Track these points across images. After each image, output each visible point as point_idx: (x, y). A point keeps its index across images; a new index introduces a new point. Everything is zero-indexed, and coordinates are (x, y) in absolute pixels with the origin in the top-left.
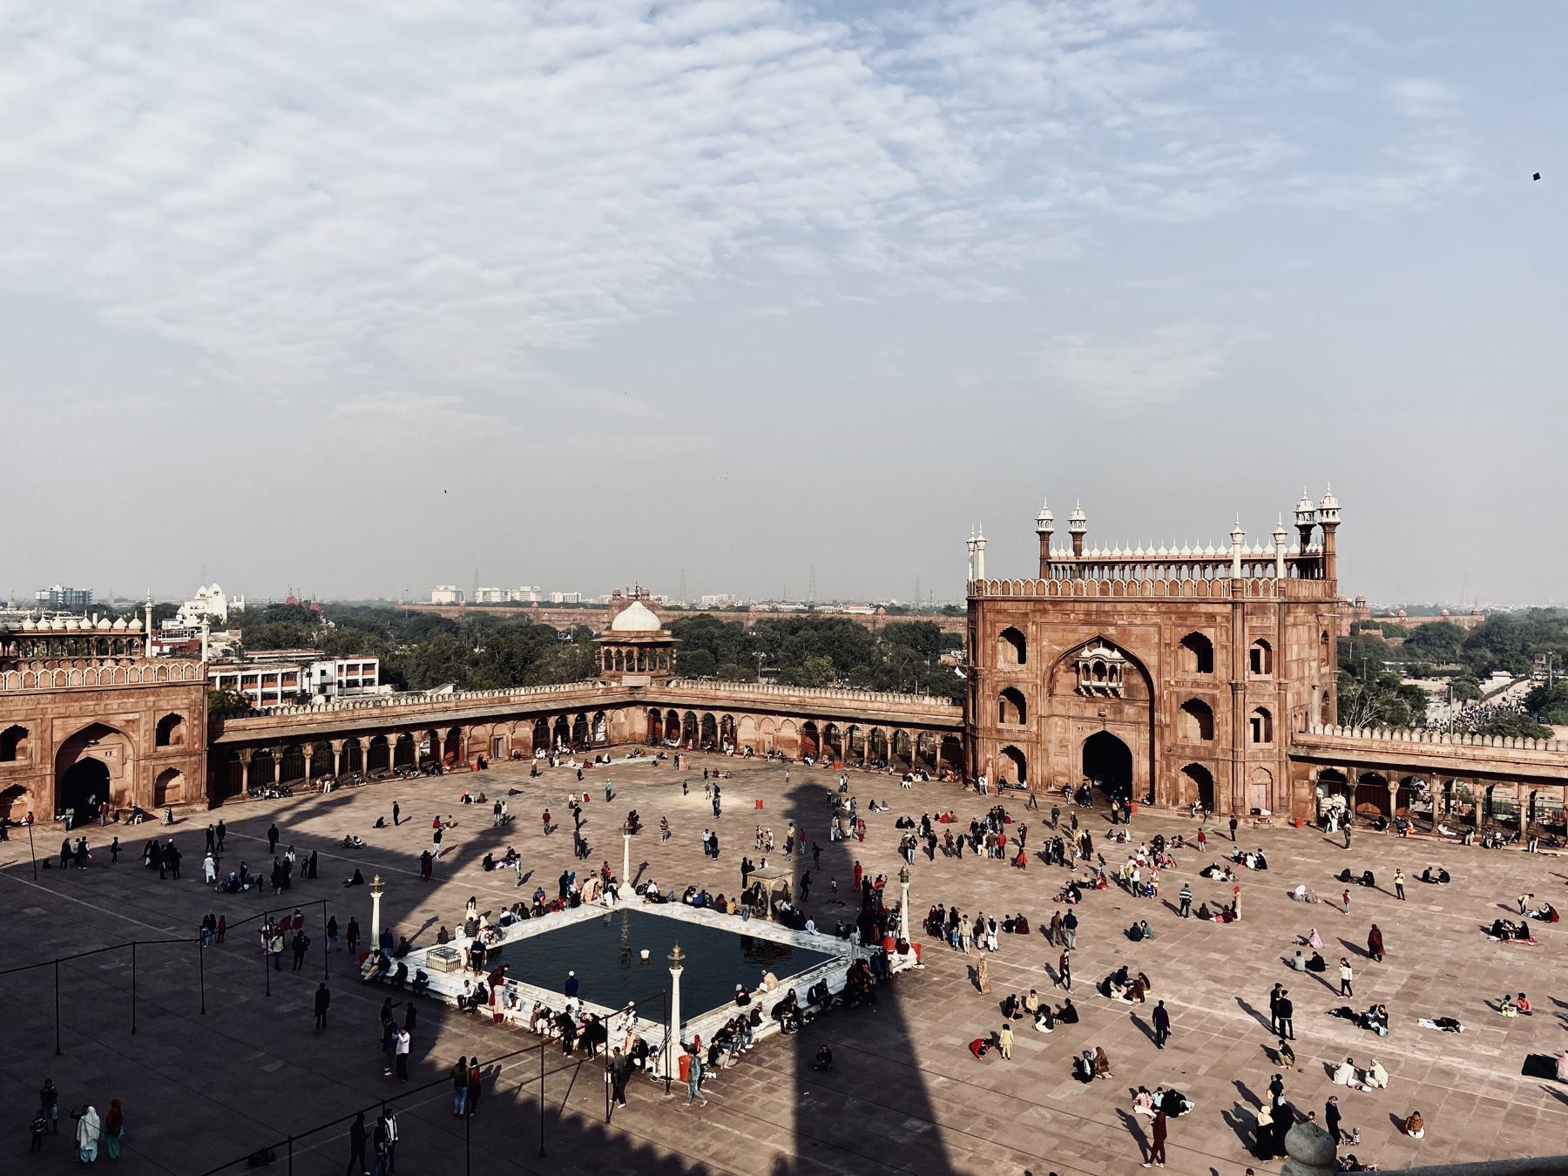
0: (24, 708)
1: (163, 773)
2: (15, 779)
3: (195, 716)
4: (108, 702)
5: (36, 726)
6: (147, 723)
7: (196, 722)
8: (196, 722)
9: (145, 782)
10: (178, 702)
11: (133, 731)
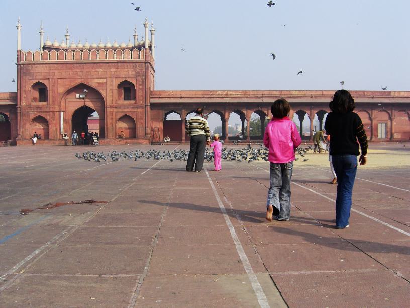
0: (44, 71)
2: (39, 112)
7: (141, 87)
8: (141, 87)
9: (111, 121)
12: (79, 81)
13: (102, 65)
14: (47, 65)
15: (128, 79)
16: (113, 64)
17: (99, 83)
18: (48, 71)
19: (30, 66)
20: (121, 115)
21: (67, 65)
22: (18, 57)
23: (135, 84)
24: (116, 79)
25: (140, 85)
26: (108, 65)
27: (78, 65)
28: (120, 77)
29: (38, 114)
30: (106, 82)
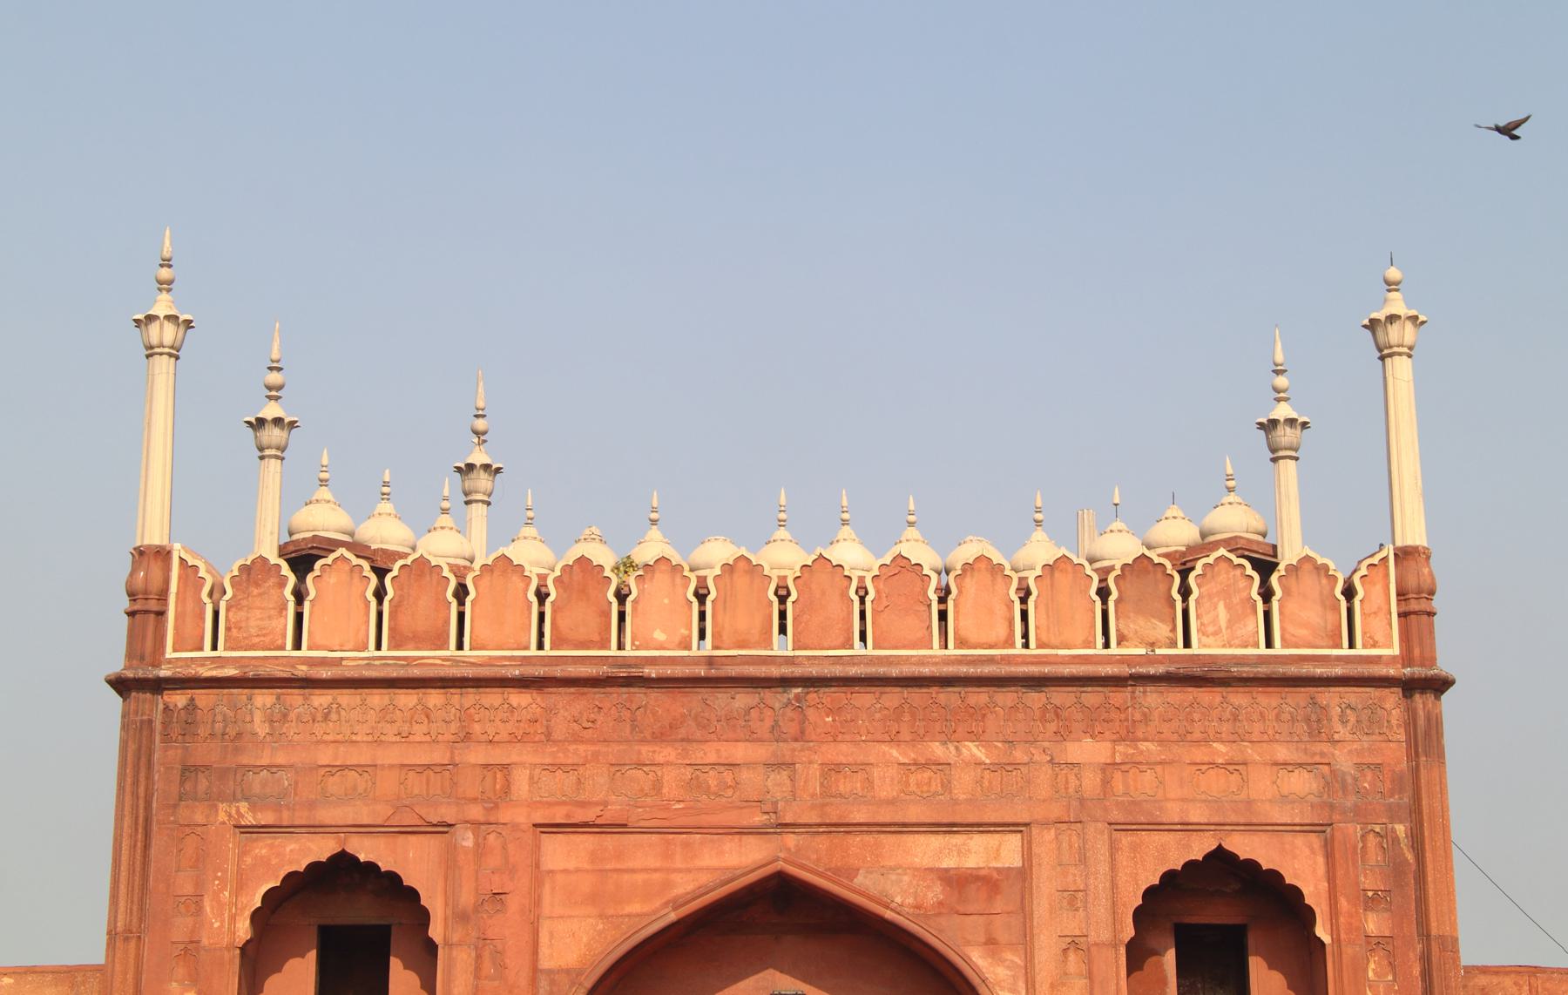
3: (1370, 882)
6: (1073, 898)
7: (1374, 924)
8: (1374, 924)
10: (1262, 785)
11: (991, 943)
13: (979, 697)
14: (435, 698)
15: (1244, 847)
16: (1092, 697)
17: (958, 881)
18: (438, 756)
19: (264, 698)
21: (639, 695)
23: (1314, 892)
24: (1126, 840)
26: (1035, 698)
27: (743, 699)
30: (1024, 874)
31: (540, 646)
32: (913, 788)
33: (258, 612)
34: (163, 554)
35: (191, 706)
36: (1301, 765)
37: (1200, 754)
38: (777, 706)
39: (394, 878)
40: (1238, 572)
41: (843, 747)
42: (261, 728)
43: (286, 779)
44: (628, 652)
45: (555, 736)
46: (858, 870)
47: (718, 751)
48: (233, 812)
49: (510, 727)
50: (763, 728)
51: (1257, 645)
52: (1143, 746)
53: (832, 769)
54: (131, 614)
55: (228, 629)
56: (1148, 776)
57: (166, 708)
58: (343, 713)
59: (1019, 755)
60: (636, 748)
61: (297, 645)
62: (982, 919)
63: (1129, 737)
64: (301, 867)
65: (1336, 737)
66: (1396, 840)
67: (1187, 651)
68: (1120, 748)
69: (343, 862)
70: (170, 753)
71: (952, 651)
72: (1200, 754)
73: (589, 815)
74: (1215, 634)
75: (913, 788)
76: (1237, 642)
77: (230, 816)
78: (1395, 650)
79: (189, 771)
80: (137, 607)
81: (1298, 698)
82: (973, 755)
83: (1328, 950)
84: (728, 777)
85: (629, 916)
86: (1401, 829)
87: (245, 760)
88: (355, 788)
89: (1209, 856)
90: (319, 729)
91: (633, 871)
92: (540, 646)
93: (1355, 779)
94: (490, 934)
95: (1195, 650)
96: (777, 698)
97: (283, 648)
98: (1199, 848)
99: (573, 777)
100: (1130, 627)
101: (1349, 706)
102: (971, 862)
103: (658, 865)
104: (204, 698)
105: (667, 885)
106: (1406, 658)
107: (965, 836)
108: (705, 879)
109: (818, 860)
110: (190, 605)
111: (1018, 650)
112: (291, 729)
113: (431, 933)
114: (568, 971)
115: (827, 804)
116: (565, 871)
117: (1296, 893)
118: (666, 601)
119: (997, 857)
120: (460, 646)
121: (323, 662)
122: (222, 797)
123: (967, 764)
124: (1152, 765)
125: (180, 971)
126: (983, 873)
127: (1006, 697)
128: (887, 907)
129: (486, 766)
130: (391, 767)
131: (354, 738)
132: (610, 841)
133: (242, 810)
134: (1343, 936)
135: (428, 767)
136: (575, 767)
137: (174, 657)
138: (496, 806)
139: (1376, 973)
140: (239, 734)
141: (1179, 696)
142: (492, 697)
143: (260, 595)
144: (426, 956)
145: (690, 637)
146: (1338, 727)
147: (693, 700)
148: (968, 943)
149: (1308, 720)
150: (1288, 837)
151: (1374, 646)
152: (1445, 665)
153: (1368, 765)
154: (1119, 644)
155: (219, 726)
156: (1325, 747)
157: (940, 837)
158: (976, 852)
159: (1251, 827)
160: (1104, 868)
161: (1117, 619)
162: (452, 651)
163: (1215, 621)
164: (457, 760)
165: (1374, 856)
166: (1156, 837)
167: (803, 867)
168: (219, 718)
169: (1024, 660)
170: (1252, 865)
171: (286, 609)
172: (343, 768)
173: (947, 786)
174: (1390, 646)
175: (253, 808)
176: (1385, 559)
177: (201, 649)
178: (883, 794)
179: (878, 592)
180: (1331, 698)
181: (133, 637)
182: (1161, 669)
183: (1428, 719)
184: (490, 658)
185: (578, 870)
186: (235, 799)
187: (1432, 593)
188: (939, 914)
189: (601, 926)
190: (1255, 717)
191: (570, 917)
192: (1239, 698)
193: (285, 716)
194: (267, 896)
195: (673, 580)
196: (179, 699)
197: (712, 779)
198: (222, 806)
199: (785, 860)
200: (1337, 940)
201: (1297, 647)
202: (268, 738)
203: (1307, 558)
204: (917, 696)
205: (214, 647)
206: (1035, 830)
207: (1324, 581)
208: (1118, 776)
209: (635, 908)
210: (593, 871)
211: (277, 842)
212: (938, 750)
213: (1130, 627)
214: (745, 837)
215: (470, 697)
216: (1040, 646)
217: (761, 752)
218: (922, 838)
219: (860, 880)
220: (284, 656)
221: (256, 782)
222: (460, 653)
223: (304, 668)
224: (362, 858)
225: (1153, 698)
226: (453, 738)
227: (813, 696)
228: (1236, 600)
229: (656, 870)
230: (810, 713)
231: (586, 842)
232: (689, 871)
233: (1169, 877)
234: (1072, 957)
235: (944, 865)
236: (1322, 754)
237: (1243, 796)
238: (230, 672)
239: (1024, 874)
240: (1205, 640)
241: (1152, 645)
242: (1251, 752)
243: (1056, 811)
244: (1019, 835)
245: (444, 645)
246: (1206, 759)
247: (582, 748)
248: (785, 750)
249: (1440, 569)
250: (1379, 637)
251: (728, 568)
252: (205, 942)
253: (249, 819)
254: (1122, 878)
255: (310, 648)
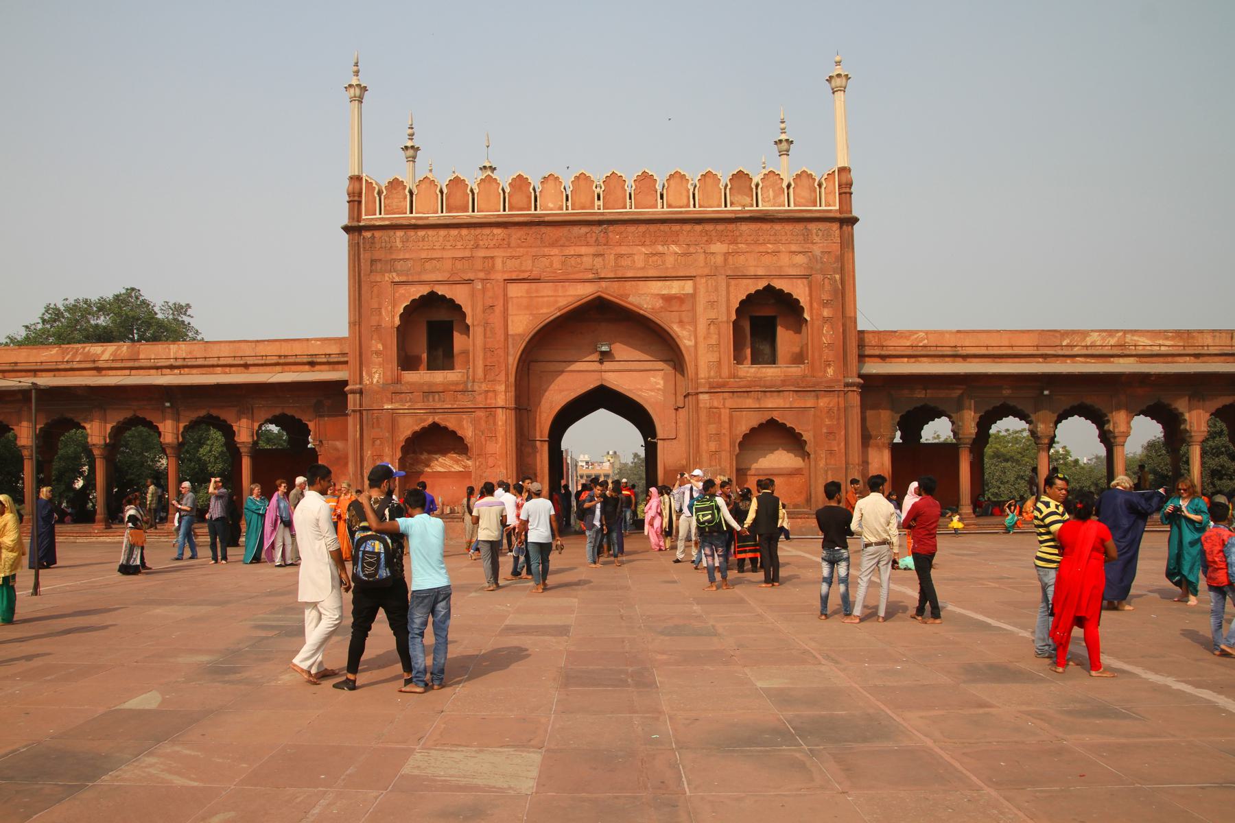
1: (753, 430)
2: (434, 411)
3: (825, 297)
4: (623, 250)
5: (473, 295)
6: (712, 304)
7: (826, 313)
8: (826, 313)
9: (713, 446)
10: (784, 260)
11: (681, 322)
12: (583, 292)
13: (676, 227)
14: (464, 232)
15: (778, 284)
16: (720, 227)
17: (668, 299)
18: (467, 254)
19: (400, 233)
20: (754, 420)
21: (543, 229)
22: (355, 200)
23: (804, 301)
24: (733, 282)
25: (826, 304)
26: (698, 228)
27: (584, 230)
28: (745, 277)
29: (430, 421)
30: (693, 296)
31: (504, 210)
32: (651, 263)
33: (396, 200)
34: (358, 179)
35: (373, 237)
36: (800, 252)
37: (762, 249)
38: (597, 232)
39: (452, 301)
40: (777, 177)
41: (623, 248)
42: (399, 244)
43: (410, 264)
44: (538, 212)
45: (511, 245)
46: (629, 295)
47: (574, 250)
48: (391, 277)
49: (494, 242)
50: (592, 241)
51: (784, 206)
52: (740, 246)
53: (620, 256)
54: (348, 202)
55: (385, 207)
56: (742, 257)
57: (364, 238)
58: (430, 238)
59: (692, 250)
60: (543, 249)
61: (411, 212)
62: (678, 313)
63: (734, 242)
64: (417, 297)
65: (814, 241)
66: (836, 281)
67: (758, 208)
68: (731, 246)
69: (432, 294)
70: (366, 255)
71: (665, 209)
72: (762, 249)
73: (525, 275)
74: (768, 201)
75: (651, 263)
76: (776, 205)
77: (389, 278)
78: (837, 207)
79: (373, 261)
80: (351, 199)
81: (799, 227)
82: (674, 250)
83: (809, 323)
84: (579, 260)
85: (542, 314)
86: (837, 277)
87: (394, 257)
88: (435, 267)
89: (765, 288)
90: (421, 244)
91: (542, 297)
92: (504, 210)
93: (821, 258)
94: (489, 321)
95: (760, 208)
96: (597, 229)
97: (406, 213)
98: (761, 285)
99: (518, 261)
100: (735, 199)
101: (819, 229)
102: (673, 291)
103: (552, 294)
104: (378, 234)
105: (556, 302)
106: (840, 211)
107: (671, 282)
108: (570, 299)
109: (614, 292)
110: (370, 197)
111: (691, 208)
112: (410, 245)
113: (467, 321)
114: (519, 335)
115: (616, 270)
116: (517, 297)
117: (797, 301)
118: (553, 191)
119: (683, 290)
120: (473, 211)
121: (421, 218)
122: (386, 271)
123: (671, 253)
124: (743, 253)
125: (375, 336)
126: (678, 295)
127: (687, 227)
128: (641, 309)
129: (484, 257)
130: (449, 258)
131: (434, 247)
132: (534, 286)
133: (394, 276)
134: (815, 317)
135: (463, 258)
136: (519, 257)
137: (366, 218)
138: (490, 273)
139: (827, 332)
140: (391, 247)
141: (753, 226)
142: (487, 231)
143: (397, 193)
144: (466, 329)
145: (563, 205)
146: (815, 237)
147: (564, 231)
148: (673, 322)
149: (804, 235)
150: (795, 280)
151: (829, 206)
152: (855, 213)
153: (826, 252)
154: (731, 205)
155: (383, 244)
156: (810, 245)
157: (661, 282)
158: (675, 288)
159: (781, 277)
160: (724, 293)
161: (730, 195)
162: (470, 213)
163: (768, 197)
164: (474, 255)
165: (827, 287)
166: (745, 281)
167: (608, 294)
168: (383, 241)
169: (694, 212)
170: (781, 291)
171: (406, 198)
172: (432, 259)
173: (664, 262)
174: (835, 206)
175: (398, 275)
176: (834, 172)
177: (375, 215)
178: (639, 266)
179: (636, 186)
180: (813, 227)
181: (351, 210)
182: (748, 215)
183: (849, 234)
184: (486, 215)
185: (521, 297)
186: (391, 272)
187: (851, 185)
188: (661, 312)
189: (531, 318)
190: (783, 234)
191: (520, 314)
192: (778, 227)
193: (408, 239)
194: (405, 308)
195: (555, 184)
196: (368, 234)
197: (573, 261)
198: (387, 275)
199: (601, 292)
200: (812, 319)
201: (800, 206)
202: (402, 249)
203: (804, 172)
204: (652, 227)
205: (380, 214)
206: (698, 279)
207: (811, 180)
208: (730, 257)
209: (544, 311)
210: (526, 297)
211: (408, 288)
212: (660, 248)
213: (735, 199)
214: (586, 283)
215: (478, 231)
216: (700, 207)
217: (591, 250)
218: (654, 282)
219: (631, 299)
220: (407, 217)
221: (399, 265)
222: (473, 214)
223: (414, 221)
224: (440, 293)
225: (744, 227)
226: (472, 247)
227: (611, 228)
228: (776, 188)
229: (552, 296)
230: (610, 234)
231: (525, 286)
232: (564, 296)
233: (749, 296)
234: (712, 327)
235: (663, 293)
236: (809, 248)
237: (778, 265)
238: (387, 223)
239: (693, 296)
240: (764, 204)
241: (744, 206)
242: (782, 248)
243: (706, 271)
244: (691, 281)
245: (467, 211)
246: (764, 251)
247: (522, 249)
248: (601, 249)
249: (854, 175)
250: (831, 203)
251: (577, 178)
252: (383, 325)
253: (397, 279)
254: (732, 297)
255: (416, 213)
